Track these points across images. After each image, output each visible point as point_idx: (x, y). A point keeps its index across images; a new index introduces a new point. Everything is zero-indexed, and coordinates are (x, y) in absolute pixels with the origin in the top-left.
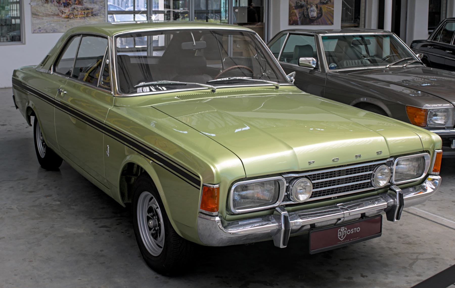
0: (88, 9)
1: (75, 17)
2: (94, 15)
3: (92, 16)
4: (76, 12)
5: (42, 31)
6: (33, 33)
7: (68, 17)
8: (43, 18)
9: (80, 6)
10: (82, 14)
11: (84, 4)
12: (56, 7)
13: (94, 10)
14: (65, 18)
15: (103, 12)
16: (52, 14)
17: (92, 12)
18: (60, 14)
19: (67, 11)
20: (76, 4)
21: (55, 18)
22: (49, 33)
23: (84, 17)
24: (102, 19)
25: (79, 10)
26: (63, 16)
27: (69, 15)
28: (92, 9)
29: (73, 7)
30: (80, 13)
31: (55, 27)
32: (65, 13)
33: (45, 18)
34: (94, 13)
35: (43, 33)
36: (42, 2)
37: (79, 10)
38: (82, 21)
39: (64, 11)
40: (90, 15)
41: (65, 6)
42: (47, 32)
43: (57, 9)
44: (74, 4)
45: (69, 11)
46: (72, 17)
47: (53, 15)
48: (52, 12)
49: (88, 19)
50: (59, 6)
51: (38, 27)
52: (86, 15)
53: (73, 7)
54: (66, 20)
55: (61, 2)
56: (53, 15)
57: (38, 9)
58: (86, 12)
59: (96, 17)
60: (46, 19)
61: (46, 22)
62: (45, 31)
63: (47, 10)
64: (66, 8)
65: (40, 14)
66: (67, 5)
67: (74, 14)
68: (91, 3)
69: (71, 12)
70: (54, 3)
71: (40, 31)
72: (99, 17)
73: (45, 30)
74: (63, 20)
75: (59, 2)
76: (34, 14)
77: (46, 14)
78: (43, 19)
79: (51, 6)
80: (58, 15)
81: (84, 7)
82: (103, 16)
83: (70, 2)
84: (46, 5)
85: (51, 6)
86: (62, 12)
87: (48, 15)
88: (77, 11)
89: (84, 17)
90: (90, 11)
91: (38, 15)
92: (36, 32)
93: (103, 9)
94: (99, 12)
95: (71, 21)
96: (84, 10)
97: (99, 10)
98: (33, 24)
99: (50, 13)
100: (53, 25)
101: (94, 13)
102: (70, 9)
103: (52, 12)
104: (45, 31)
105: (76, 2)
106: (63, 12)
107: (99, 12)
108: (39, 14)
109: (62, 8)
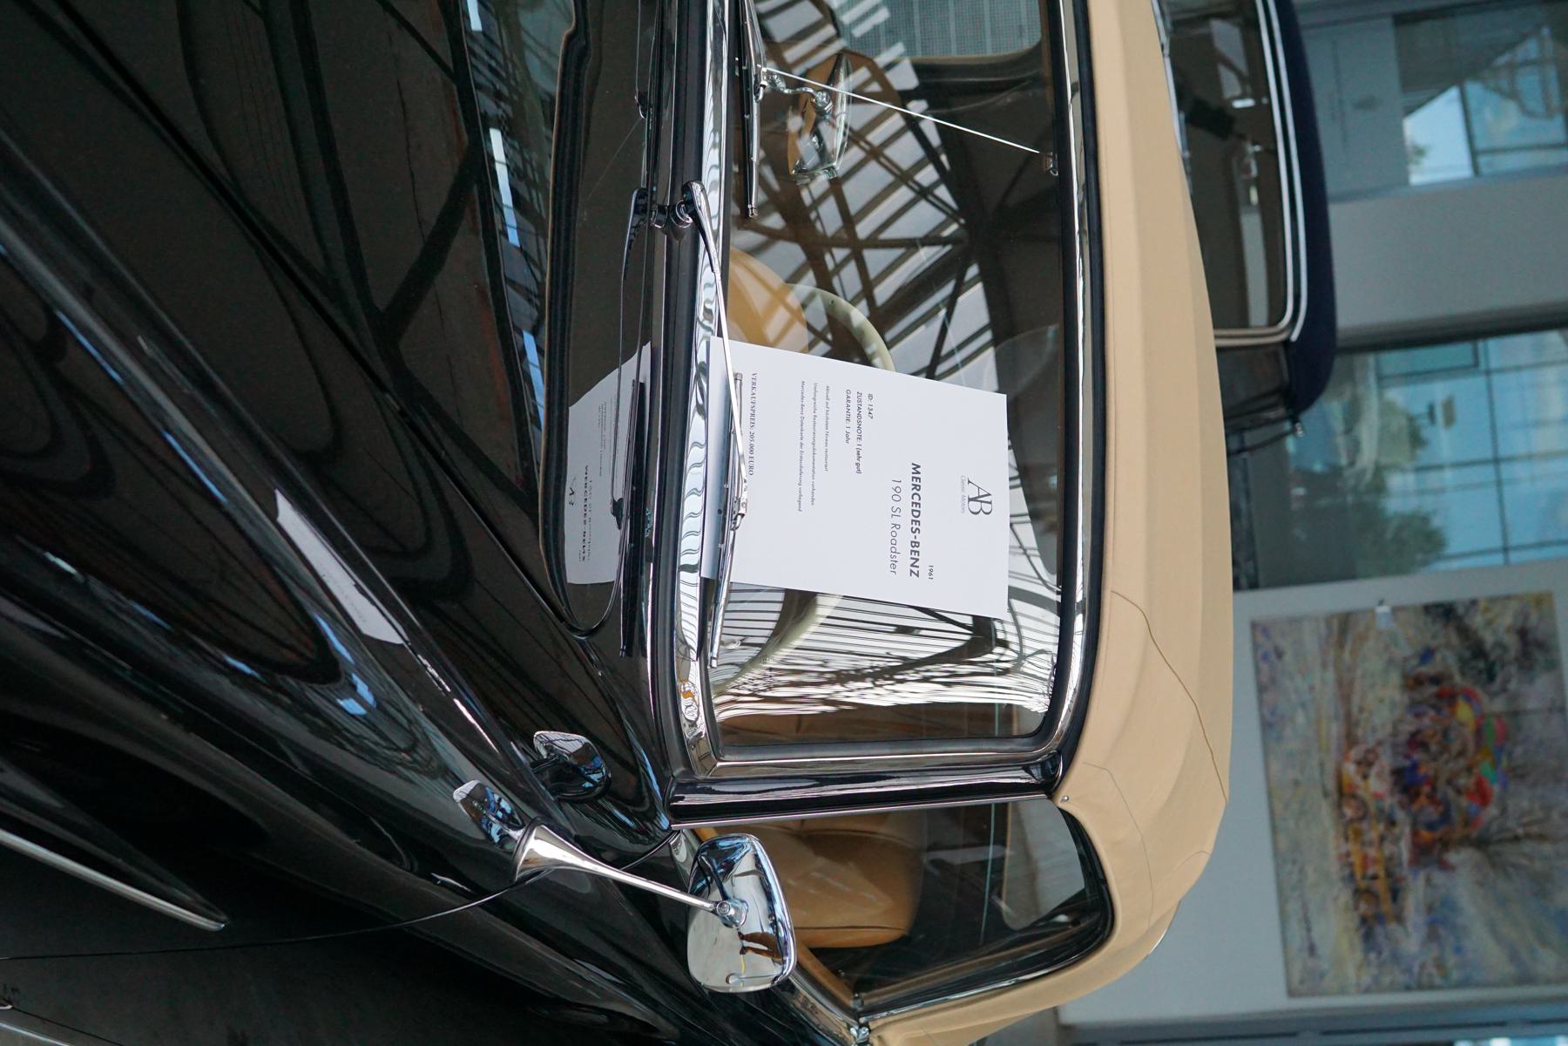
0: (1395, 894)
1: (1351, 830)
2: (1369, 928)
3: (1364, 920)
4: (1373, 835)
5: (1265, 667)
6: (1254, 626)
7: (1343, 793)
8: (1331, 669)
9: (1404, 849)
10: (1365, 866)
11: (1422, 876)
12: (1389, 729)
13: (1393, 926)
15: (1386, 980)
16: (1355, 710)
17: (1380, 919)
18: (1355, 753)
19: (1377, 785)
20: (1415, 834)
21: (1335, 729)
22: (1261, 702)
23: (1352, 876)
24: (1351, 972)
25: (1388, 849)
26: (1350, 769)
27: (1354, 796)
28: (1399, 919)
29: (1400, 815)
30: (1372, 852)
31: (1288, 732)
32: (1365, 777)
33: (1330, 675)
34: (1379, 930)
35: (1258, 671)
36: (1406, 660)
37: (1388, 849)
38: (1334, 868)
39: (1374, 771)
40: (1363, 907)
41: (1397, 773)
42: (1262, 689)
43: (1380, 735)
44: (1414, 824)
45: (1377, 797)
46: (1349, 812)
47: (1348, 715)
48: (1361, 710)
49: (1345, 896)
50: (1395, 746)
51: (1285, 644)
52: (1363, 884)
53: (1400, 815)
54: (1331, 785)
55: (1418, 756)
56: (1348, 715)
57: (1371, 643)
58: (1380, 886)
60: (1324, 682)
61: (1313, 683)
62: (1265, 679)
63: (1373, 686)
64: (1389, 779)
65: (1347, 656)
66: (1407, 782)
67: (1364, 825)
68: (1430, 909)
69: (1372, 808)
70: (1410, 717)
71: (1265, 657)
72: (1359, 955)
73: (1273, 681)
74: (1330, 768)
75: (1416, 741)
76: (1344, 626)
77: (1351, 683)
78: (1324, 665)
79: (1393, 705)
80: (1350, 740)
81: (1405, 871)
82: (1366, 979)
83: (1423, 800)
84: (1395, 678)
85: (1393, 705)
86: (1365, 764)
87: (1345, 690)
88: (1382, 839)
89: (1352, 876)
90: (1386, 907)
91: (1341, 645)
92: (1261, 639)
93: (1402, 978)
94: (1386, 954)
95: (1325, 811)
96: (1389, 874)
97: (1396, 957)
98: (1295, 622)
99: (1356, 699)
100: (1300, 718)
101: (1379, 930)
102: (1390, 802)
103: (1361, 710)
104: (1265, 679)
105: (1425, 835)
106: (1370, 764)
108: (1348, 647)
109: (1386, 761)
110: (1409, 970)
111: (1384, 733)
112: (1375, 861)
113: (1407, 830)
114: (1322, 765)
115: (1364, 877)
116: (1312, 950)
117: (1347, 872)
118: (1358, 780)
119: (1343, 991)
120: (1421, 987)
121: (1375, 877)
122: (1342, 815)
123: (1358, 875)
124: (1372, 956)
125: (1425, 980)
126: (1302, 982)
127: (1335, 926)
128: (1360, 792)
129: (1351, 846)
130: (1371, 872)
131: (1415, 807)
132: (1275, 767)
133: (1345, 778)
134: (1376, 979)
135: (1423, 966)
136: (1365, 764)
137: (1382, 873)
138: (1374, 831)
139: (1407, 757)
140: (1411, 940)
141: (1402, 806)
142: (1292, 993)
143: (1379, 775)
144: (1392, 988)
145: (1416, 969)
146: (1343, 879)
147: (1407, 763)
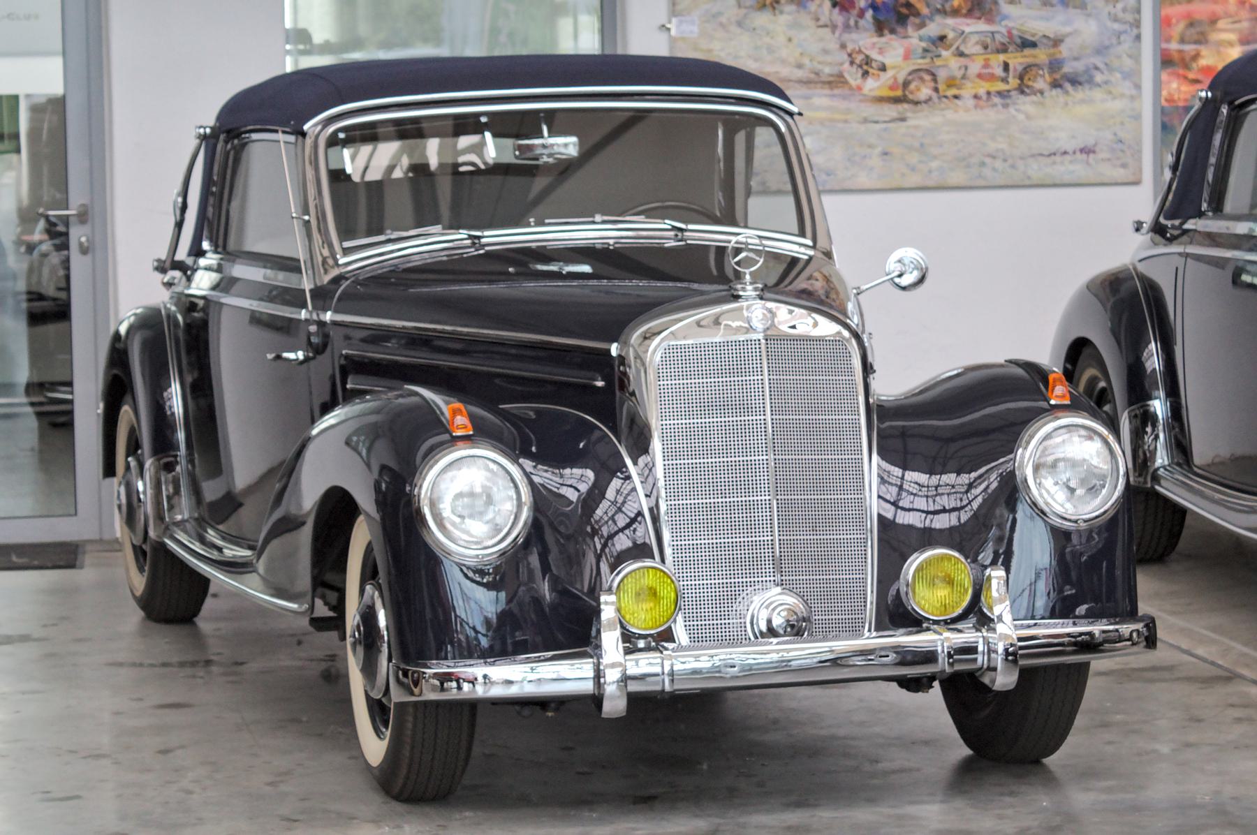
0: (1027, 44)
1: (947, 91)
2: (1064, 80)
3: (1056, 85)
4: (955, 64)
7: (901, 97)
9: (975, 27)
13: (1064, 51)
14: (881, 100)
15: (1128, 63)
16: (800, 74)
17: (1055, 65)
19: (896, 53)
24: (1117, 105)
25: (972, 47)
26: (872, 85)
27: (906, 84)
28: (1057, 42)
29: (933, 29)
30: (975, 67)
32: (883, 68)
34: (1067, 69)
37: (972, 47)
38: (991, 115)
39: (874, 55)
40: (1040, 84)
41: (880, 28)
43: (833, 45)
45: (907, 57)
46: (925, 92)
49: (1026, 104)
50: (847, 27)
52: (1013, 82)
53: (933, 29)
54: (891, 111)
58: (1017, 60)
59: (1079, 94)
63: (770, 50)
64: (888, 37)
67: (942, 75)
72: (1097, 94)
74: (870, 110)
79: (795, 25)
80: (837, 81)
81: (1000, 28)
82: (1126, 87)
84: (762, 19)
86: (866, 66)
88: (962, 55)
89: (1000, 94)
90: (1041, 55)
93: (1127, 44)
94: (1098, 61)
95: (921, 120)
96: (1003, 49)
97: (1101, 50)
101: (1067, 69)
102: (915, 38)
103: (800, 66)
106: (868, 61)
107: (1098, 61)
109: (865, 40)
110: (1119, 35)
111: (830, 40)
112: (986, 66)
113: (950, 21)
114: (866, 121)
115: (1005, 80)
116: (1087, 151)
117: (997, 100)
118: (886, 77)
119: (1137, 117)
120: (1137, 24)
121: (1006, 67)
122: (928, 101)
123: (1002, 87)
124: (1099, 78)
125: (1129, 17)
126: (1124, 166)
127: (1060, 119)
128: (901, 78)
129: (967, 92)
130: (999, 71)
131: (925, 11)
132: (863, 180)
133: (887, 93)
134: (1127, 76)
135: (1116, 20)
136: (866, 66)
137: (1002, 57)
138: (949, 64)
139: (861, 14)
140: (1081, 31)
141: (922, 25)
142: (1137, 183)
143: (881, 51)
144: (1136, 58)
145: (1116, 26)
146: (1006, 106)
147: (869, 14)
